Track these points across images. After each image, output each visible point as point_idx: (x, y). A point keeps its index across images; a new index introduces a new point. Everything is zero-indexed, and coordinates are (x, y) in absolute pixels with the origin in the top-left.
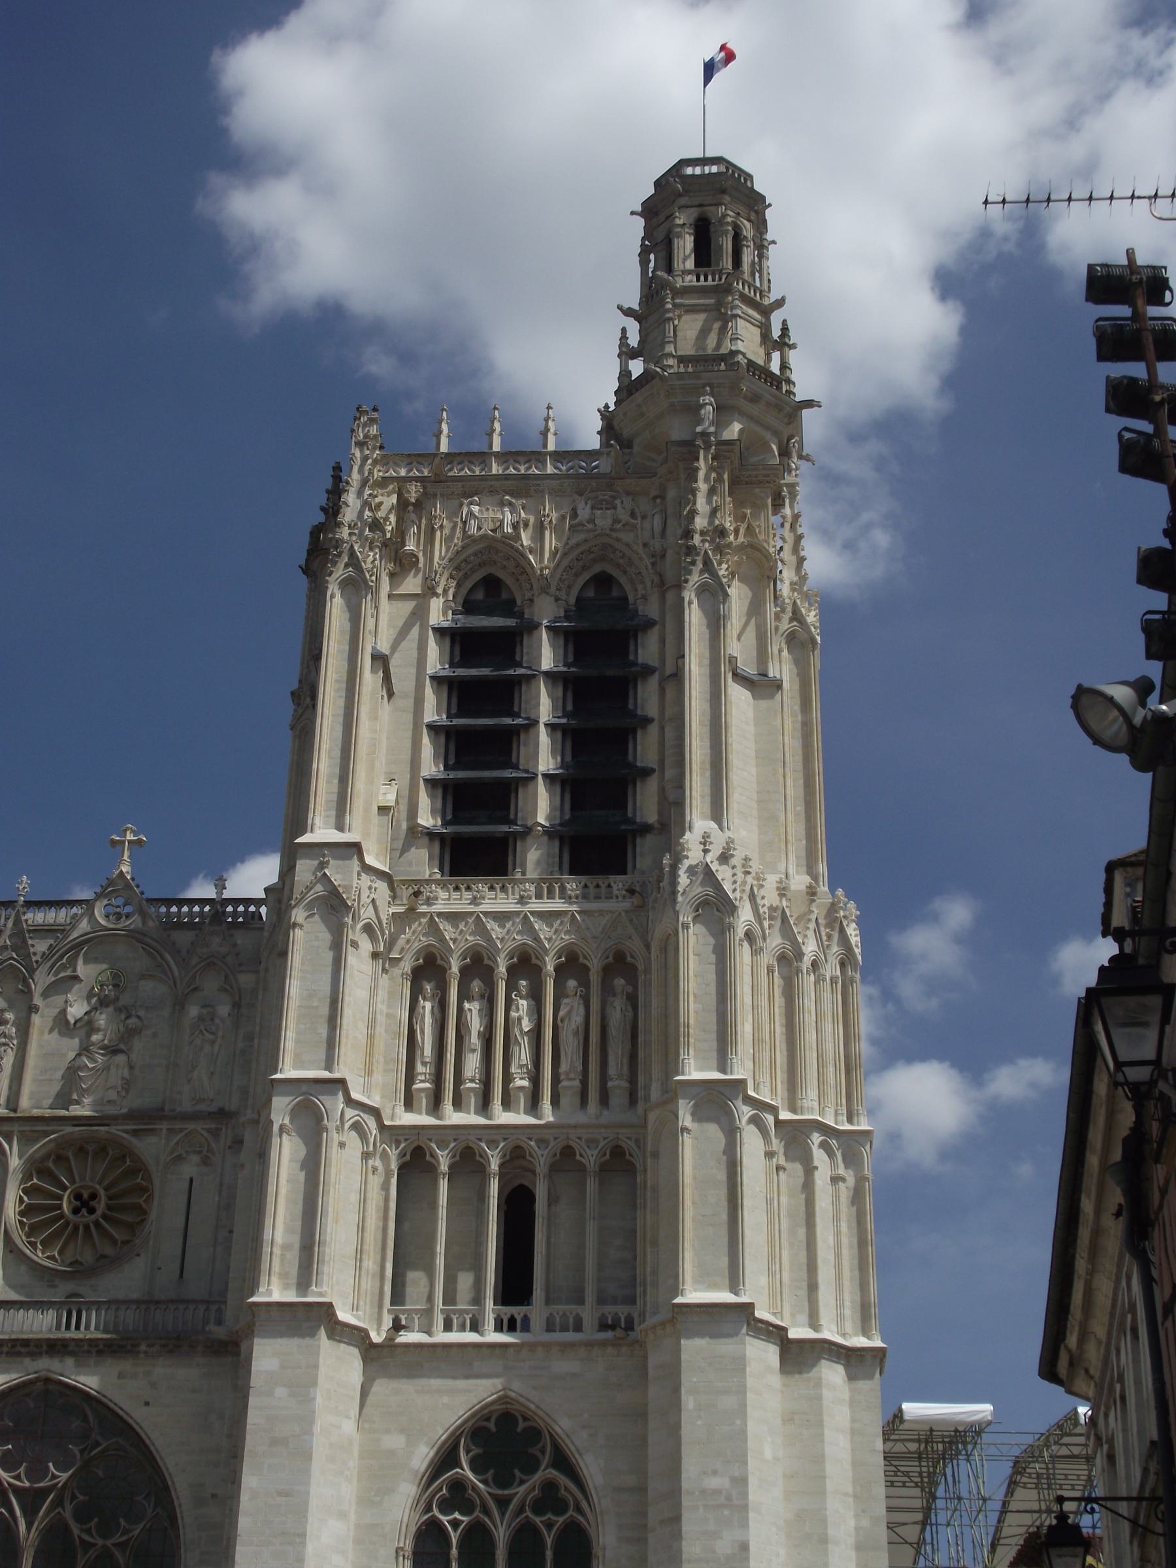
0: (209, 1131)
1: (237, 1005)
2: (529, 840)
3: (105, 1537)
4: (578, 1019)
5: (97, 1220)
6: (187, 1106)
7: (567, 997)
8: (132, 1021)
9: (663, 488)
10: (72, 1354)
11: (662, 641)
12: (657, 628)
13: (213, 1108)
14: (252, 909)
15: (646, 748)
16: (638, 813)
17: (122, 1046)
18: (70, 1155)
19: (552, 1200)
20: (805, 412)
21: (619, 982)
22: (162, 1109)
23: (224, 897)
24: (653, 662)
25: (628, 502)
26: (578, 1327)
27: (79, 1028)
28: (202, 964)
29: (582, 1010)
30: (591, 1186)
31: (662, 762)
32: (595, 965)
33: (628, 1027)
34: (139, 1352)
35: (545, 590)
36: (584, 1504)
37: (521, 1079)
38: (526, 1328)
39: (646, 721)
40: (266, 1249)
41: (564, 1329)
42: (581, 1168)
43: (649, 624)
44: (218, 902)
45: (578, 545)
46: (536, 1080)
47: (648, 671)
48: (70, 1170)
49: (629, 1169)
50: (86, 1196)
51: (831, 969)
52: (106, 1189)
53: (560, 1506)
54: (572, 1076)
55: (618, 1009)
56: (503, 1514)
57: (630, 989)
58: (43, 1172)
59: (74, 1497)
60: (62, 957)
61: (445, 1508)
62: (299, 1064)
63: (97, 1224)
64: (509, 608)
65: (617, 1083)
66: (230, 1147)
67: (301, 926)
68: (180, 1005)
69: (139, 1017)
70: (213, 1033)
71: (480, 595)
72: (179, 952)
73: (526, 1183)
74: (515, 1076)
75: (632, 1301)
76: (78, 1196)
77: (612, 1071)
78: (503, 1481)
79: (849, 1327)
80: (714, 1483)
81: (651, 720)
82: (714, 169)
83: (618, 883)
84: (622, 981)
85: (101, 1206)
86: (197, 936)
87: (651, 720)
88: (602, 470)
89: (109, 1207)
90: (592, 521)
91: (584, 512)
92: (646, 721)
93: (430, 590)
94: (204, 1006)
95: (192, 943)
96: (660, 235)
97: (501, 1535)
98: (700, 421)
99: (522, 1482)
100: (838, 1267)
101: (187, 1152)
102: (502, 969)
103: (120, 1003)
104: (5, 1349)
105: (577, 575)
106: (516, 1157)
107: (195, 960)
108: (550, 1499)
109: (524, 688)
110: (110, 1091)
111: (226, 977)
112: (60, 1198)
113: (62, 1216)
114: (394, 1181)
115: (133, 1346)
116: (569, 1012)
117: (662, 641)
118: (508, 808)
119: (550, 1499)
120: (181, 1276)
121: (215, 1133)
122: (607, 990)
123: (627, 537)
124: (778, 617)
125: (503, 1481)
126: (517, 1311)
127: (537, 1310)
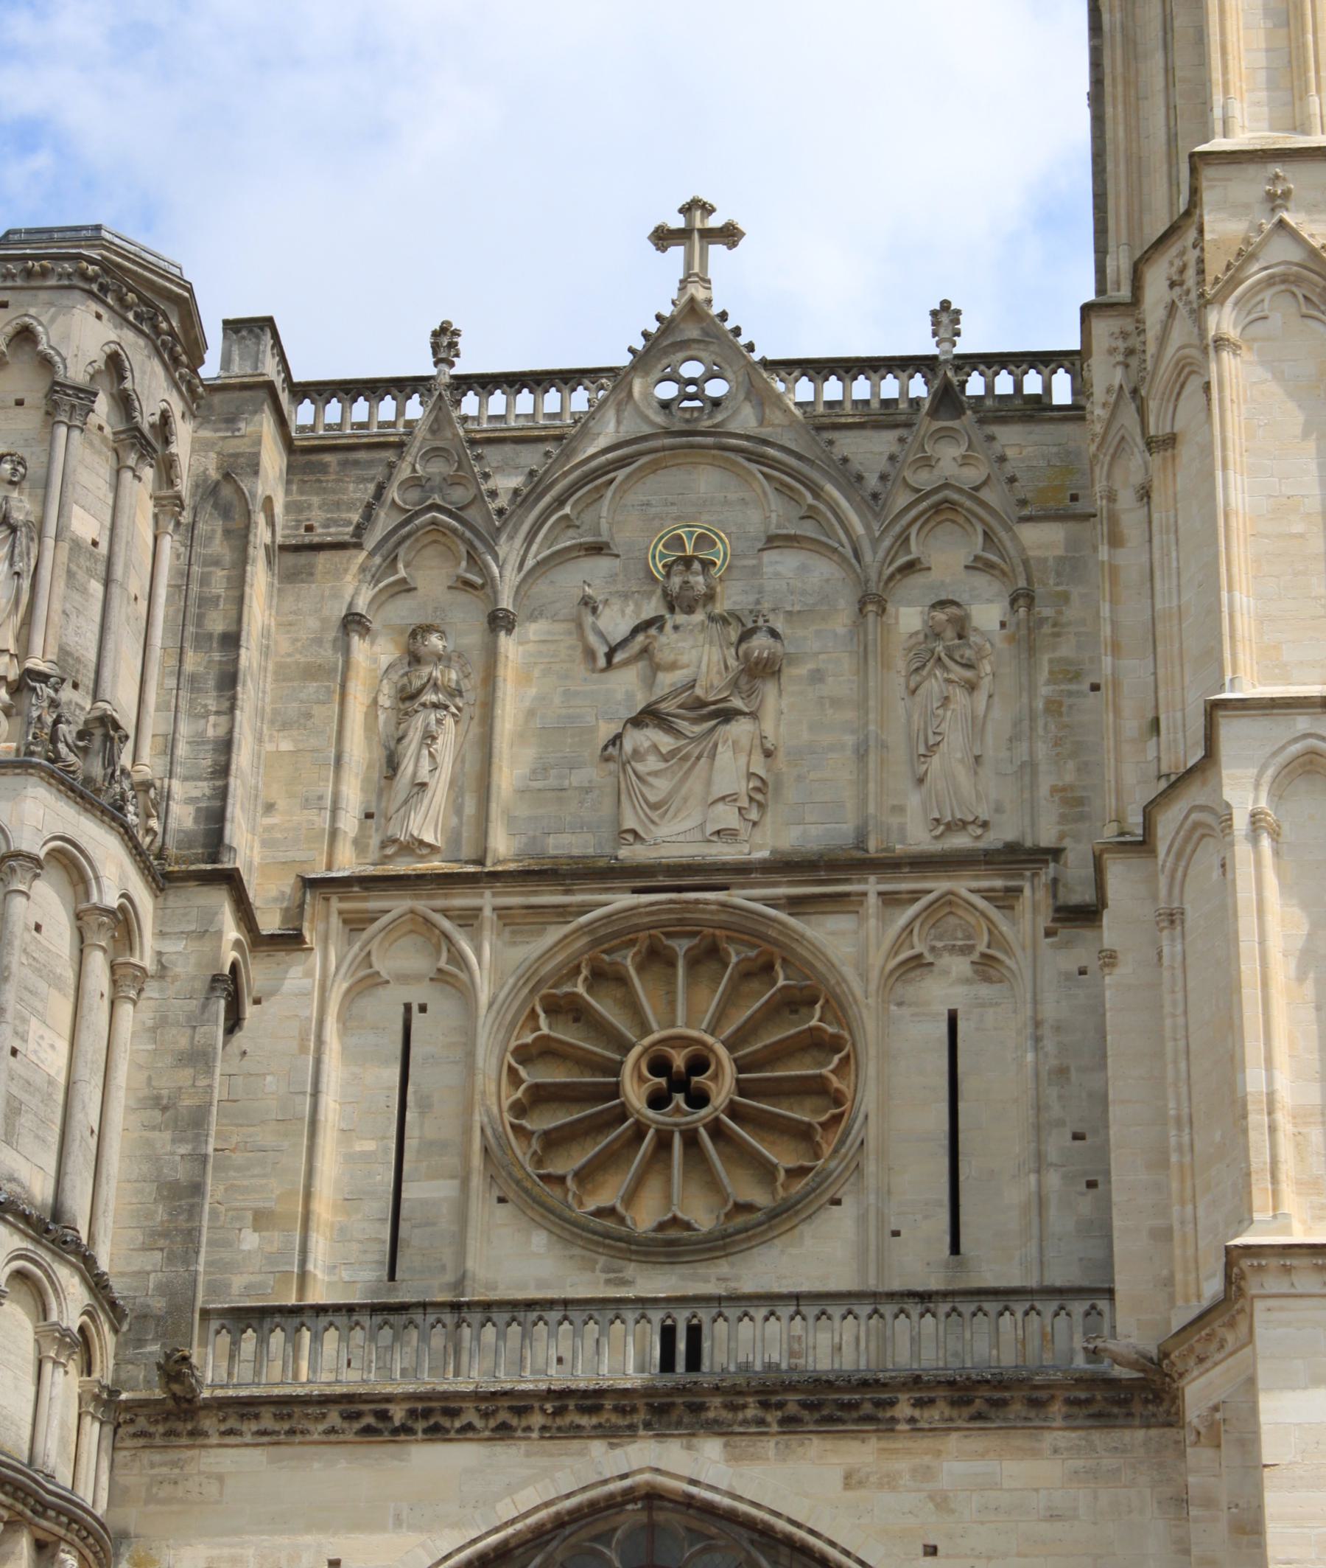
0: (988, 895)
1: (1022, 598)
5: (717, 1119)
6: (919, 838)
8: (760, 644)
10: (716, 1428)
13: (993, 839)
14: (1033, 383)
17: (737, 703)
18: (628, 961)
22: (861, 843)
23: (958, 350)
27: (626, 663)
28: (924, 504)
34: (893, 1420)
40: (1257, 1119)
44: (946, 361)
50: (679, 1060)
52: (731, 1045)
60: (560, 502)
63: (717, 1130)
66: (1049, 933)
67: (1235, 348)
69: (774, 634)
70: (969, 666)
72: (860, 478)
76: (659, 1065)
85: (722, 1090)
86: (902, 440)
89: (742, 1088)
94: (942, 604)
95: (892, 458)
101: (933, 949)
103: (719, 608)
104: (537, 1420)
110: (720, 807)
111: (985, 533)
112: (615, 1069)
113: (622, 1114)
115: (879, 1404)
120: (955, 1248)
121: (1006, 899)
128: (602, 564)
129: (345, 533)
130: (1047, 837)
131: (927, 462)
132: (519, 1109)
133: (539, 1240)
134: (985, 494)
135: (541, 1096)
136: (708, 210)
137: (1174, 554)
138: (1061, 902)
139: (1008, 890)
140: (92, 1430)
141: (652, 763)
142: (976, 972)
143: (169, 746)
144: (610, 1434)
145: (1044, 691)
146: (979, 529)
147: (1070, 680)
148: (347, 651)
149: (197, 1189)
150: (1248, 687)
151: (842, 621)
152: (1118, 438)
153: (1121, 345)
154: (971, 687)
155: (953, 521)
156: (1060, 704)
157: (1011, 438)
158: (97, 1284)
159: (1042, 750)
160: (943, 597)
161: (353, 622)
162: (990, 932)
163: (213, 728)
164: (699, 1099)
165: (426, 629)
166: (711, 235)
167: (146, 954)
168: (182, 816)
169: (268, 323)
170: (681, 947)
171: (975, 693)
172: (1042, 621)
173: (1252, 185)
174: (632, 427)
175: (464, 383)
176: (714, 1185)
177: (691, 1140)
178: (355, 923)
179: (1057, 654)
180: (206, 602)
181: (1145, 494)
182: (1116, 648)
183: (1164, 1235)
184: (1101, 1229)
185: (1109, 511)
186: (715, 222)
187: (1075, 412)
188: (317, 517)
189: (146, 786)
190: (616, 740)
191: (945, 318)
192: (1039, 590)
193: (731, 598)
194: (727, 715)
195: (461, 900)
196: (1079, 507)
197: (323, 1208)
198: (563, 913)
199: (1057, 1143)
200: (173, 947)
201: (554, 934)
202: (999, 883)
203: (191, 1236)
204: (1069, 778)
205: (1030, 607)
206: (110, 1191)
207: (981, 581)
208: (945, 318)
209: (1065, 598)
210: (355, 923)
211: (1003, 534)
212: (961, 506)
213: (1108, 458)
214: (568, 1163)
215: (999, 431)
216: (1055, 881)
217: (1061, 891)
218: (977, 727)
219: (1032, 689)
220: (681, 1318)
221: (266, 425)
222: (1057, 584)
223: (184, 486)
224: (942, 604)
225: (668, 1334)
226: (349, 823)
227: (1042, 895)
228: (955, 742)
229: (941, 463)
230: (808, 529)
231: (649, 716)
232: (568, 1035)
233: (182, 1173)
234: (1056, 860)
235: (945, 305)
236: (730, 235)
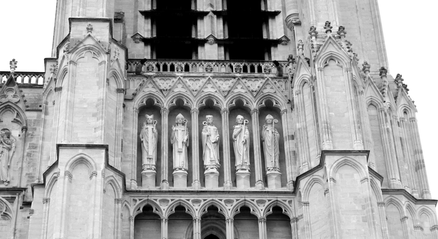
0: (7, 199)
1: (25, 129)
2: (207, 46)
4: (245, 135)
7: (237, 124)
13: (10, 186)
16: (271, 35)
21: (269, 117)
23: (16, 71)
29: (247, 131)
33: (277, 142)
37: (211, 168)
42: (254, 219)
44: (12, 73)
46: (221, 170)
51: (400, 114)
54: (244, 167)
55: (270, 132)
65: (273, 172)
66: (21, 208)
73: (214, 233)
74: (207, 167)
77: (269, 165)
84: (271, 117)
102: (195, 106)
111: (17, 113)
114: (132, 223)
116: (240, 132)
121: (12, 200)
130: (23, 186)
131: (5, 96)
134: (19, 105)
137: (58, 115)
138: (25, 200)
139: (12, 198)
142: (2, 217)
145: (27, 151)
146: (16, 112)
147: (34, 148)
152: (50, 90)
153: (53, 68)
154: (9, 149)
155: (10, 111)
156: (31, 154)
157: (26, 91)
159: (25, 165)
160: (5, 128)
162: (6, 207)
171: (10, 151)
172: (29, 134)
179: (31, 142)
182: (43, 138)
185: (45, 107)
192: (29, 127)
196: (41, 108)
202: (10, 196)
204: (31, 171)
205: (26, 131)
207: (15, 125)
208: (13, 62)
209: (35, 129)
211: (21, 114)
212: (12, 107)
213: (47, 94)
215: (23, 89)
216: (24, 196)
217: (25, 198)
218: (10, 159)
219: (24, 150)
222: (34, 126)
224: (4, 130)
227: (20, 199)
229: (8, 97)
234: (25, 191)
235: (14, 60)
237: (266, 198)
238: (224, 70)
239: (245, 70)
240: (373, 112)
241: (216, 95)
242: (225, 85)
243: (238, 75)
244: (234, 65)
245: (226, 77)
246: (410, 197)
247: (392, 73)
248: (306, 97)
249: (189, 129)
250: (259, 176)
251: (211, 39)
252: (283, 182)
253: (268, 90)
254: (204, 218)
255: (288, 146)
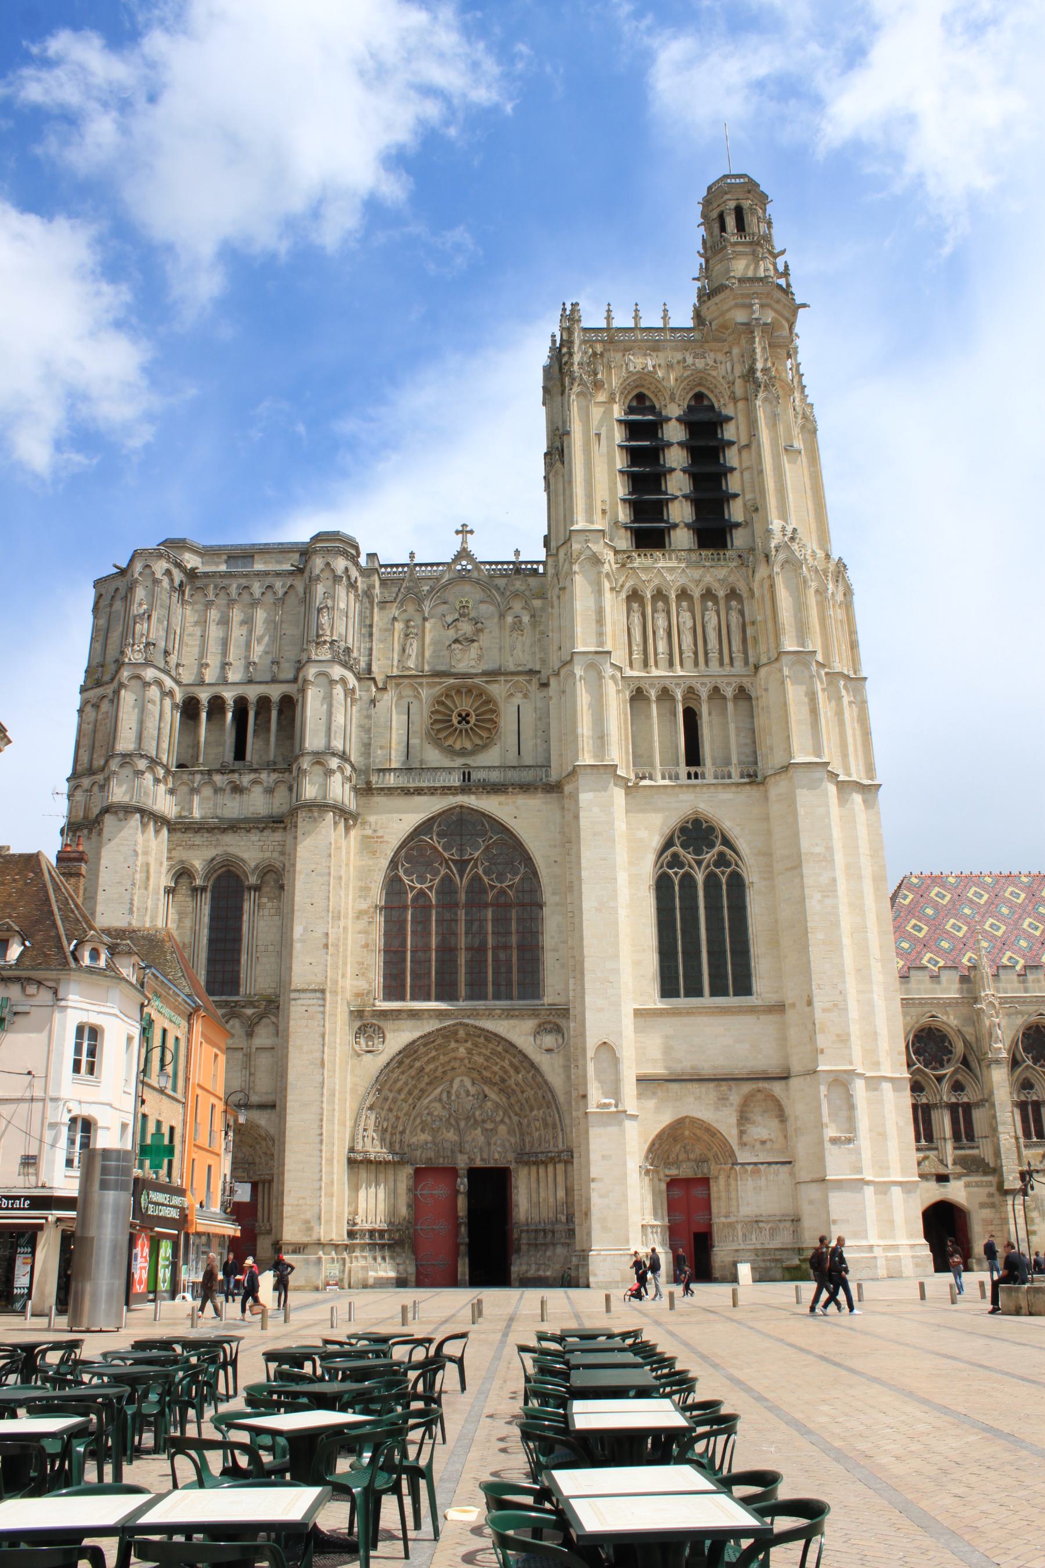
1: (533, 616)
3: (501, 882)
6: (512, 668)
8: (479, 625)
9: (731, 347)
10: (474, 793)
11: (738, 428)
12: (733, 421)
13: (527, 668)
14: (535, 566)
15: (733, 483)
19: (710, 714)
20: (800, 310)
21: (734, 603)
24: (733, 439)
25: (712, 355)
26: (730, 777)
30: (730, 705)
31: (743, 490)
32: (721, 594)
35: (672, 399)
36: (740, 862)
38: (703, 777)
39: (732, 470)
40: (580, 739)
41: (723, 778)
42: (724, 698)
43: (729, 419)
45: (688, 377)
46: (696, 653)
47: (731, 443)
48: (454, 702)
49: (749, 698)
50: (464, 714)
51: (840, 597)
53: (728, 864)
56: (699, 868)
57: (739, 607)
58: (440, 703)
59: (482, 864)
61: (670, 866)
62: (585, 645)
63: (471, 729)
64: (652, 409)
68: (502, 616)
71: (634, 404)
75: (756, 763)
76: (460, 715)
77: (734, 649)
78: (698, 852)
79: (863, 774)
80: (817, 850)
81: (735, 469)
82: (742, 180)
83: (728, 553)
85: (473, 720)
87: (735, 469)
88: (697, 337)
89: (477, 720)
90: (694, 364)
91: (690, 360)
92: (732, 470)
93: (612, 400)
96: (715, 214)
97: (700, 878)
98: (753, 312)
99: (707, 853)
100: (855, 745)
102: (673, 596)
103: (471, 616)
105: (687, 393)
106: (691, 692)
107: (508, 593)
108: (722, 861)
109: (666, 451)
112: (451, 716)
113: (453, 725)
117: (738, 428)
118: (662, 514)
119: (722, 861)
121: (529, 682)
122: (728, 609)
123: (714, 373)
124: (796, 417)
125: (698, 852)
126: (699, 770)
127: (709, 766)
128: (446, 606)
129: (392, 599)
130: (537, 668)
132: (432, 724)
133: (437, 752)
135: (436, 721)
136: (466, 526)
140: (352, 794)
141: (457, 651)
143: (359, 649)
144: (453, 794)
148: (393, 625)
149: (370, 744)
150: (580, 648)
151: (496, 620)
158: (352, 766)
159: (537, 650)
161: (395, 619)
163: (368, 645)
164: (468, 722)
165: (408, 621)
166: (468, 532)
167: (357, 696)
168: (363, 665)
169: (375, 554)
170: (464, 690)
173: (582, 537)
174: (452, 575)
175: (416, 565)
176: (471, 740)
177: (466, 730)
178: (398, 685)
180: (366, 617)
181: (559, 597)
183: (561, 755)
184: (548, 751)
186: (468, 529)
187: (545, 574)
188: (386, 595)
189: (355, 659)
190: (450, 645)
191: (517, 553)
193: (473, 614)
194: (473, 641)
195: (419, 680)
197: (393, 745)
198: (440, 683)
199: (540, 733)
200: (363, 693)
201: (438, 688)
203: (369, 754)
206: (353, 746)
207: (525, 612)
208: (517, 553)
210: (398, 685)
214: (442, 735)
218: (523, 644)
220: (467, 771)
221: (376, 577)
223: (360, 592)
225: (464, 773)
226: (395, 663)
228: (519, 646)
230: (488, 599)
231: (456, 641)
232: (441, 709)
233: (366, 741)
236: (471, 532)
237: (734, 679)
238: (694, 556)
239: (713, 560)
240: (819, 598)
241: (690, 584)
242: (697, 574)
243: (707, 564)
244: (703, 553)
245: (698, 567)
246: (847, 678)
247: (835, 556)
248: (766, 592)
249: (668, 613)
250: (726, 660)
251: (682, 525)
252: (746, 662)
253: (731, 579)
254: (684, 699)
255: (749, 631)
